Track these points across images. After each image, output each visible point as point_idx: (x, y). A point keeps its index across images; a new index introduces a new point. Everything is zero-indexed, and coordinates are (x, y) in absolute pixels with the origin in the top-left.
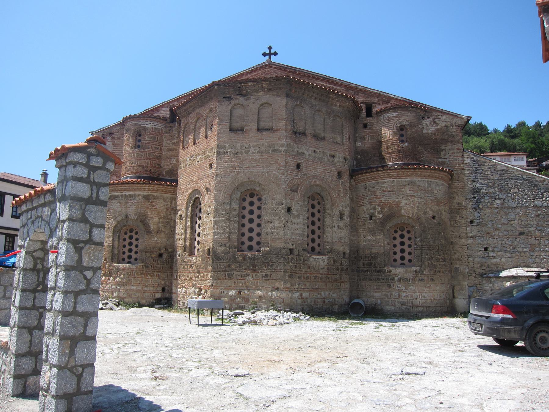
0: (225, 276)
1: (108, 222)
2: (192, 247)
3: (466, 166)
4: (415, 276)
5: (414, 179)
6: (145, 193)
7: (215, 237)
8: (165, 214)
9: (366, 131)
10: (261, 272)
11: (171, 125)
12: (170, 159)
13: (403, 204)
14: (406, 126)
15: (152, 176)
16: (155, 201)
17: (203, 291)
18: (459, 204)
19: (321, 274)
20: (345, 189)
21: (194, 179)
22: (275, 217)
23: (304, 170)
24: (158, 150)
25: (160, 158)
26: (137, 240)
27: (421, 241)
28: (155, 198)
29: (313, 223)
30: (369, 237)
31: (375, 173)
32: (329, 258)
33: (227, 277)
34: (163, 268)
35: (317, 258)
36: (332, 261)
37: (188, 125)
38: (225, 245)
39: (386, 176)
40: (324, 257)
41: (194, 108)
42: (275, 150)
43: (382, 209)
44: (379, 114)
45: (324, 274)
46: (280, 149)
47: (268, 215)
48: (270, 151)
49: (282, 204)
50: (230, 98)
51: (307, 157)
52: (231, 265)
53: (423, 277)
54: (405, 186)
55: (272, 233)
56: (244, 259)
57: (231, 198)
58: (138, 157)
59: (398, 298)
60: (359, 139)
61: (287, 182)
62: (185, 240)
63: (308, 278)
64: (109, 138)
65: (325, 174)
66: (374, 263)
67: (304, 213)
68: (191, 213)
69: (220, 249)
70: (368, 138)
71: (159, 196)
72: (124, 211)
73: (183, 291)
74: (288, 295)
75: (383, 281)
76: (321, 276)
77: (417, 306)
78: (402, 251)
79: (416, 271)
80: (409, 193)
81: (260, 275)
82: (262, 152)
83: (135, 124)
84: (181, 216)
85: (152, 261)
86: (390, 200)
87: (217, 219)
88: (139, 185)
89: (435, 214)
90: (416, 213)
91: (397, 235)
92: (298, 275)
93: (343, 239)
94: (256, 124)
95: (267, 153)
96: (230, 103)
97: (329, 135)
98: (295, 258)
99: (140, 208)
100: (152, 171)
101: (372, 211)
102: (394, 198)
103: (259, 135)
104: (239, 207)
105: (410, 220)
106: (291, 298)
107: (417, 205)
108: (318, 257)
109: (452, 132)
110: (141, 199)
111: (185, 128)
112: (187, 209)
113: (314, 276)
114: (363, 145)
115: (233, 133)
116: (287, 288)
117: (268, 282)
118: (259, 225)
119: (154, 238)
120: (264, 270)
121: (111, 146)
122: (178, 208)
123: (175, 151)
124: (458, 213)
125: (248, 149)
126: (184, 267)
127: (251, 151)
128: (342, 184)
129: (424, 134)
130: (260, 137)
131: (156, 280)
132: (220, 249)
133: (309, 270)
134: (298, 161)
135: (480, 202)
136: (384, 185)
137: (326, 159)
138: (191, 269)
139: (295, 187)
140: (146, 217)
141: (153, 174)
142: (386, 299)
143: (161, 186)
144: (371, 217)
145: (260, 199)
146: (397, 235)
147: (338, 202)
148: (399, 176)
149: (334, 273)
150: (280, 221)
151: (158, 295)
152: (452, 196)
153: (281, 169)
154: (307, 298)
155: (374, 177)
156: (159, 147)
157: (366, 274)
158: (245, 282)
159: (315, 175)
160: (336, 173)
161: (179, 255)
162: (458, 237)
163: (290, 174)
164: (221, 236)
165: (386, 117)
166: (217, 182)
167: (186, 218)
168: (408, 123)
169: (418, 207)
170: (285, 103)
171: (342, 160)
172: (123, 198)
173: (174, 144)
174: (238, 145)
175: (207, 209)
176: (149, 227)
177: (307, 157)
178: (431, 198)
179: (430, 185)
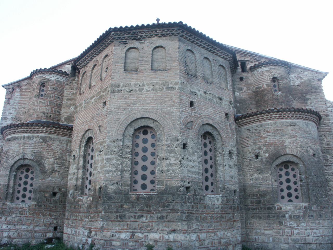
0: (117, 218)
1: (6, 162)
3: (329, 113)
4: (305, 212)
5: (295, 120)
6: (43, 135)
7: (107, 175)
8: (60, 155)
9: (243, 83)
10: (156, 213)
11: (72, 78)
12: (69, 107)
13: (287, 143)
14: (278, 78)
15: (52, 121)
16: (52, 142)
18: (328, 144)
19: (216, 214)
20: (232, 130)
22: (170, 153)
23: (197, 110)
24: (58, 99)
25: (60, 106)
26: (32, 179)
27: (307, 178)
28: (51, 139)
29: (206, 162)
30: (256, 176)
32: (223, 197)
33: (119, 219)
34: (55, 207)
35: (212, 197)
36: (225, 200)
37: (85, 74)
38: (117, 183)
40: (218, 196)
41: (91, 58)
42: (168, 88)
43: (268, 148)
44: (253, 70)
45: (219, 213)
46: (174, 86)
47: (163, 152)
48: (165, 89)
49: (178, 141)
50: (125, 43)
51: (199, 97)
52: (123, 205)
53: (312, 213)
54: (287, 126)
55: (168, 171)
57: (124, 135)
58: (41, 104)
59: (290, 236)
60: (237, 90)
61: (182, 119)
62: (77, 179)
63: (204, 219)
64: (18, 90)
65: (215, 115)
66: (262, 201)
67: (199, 151)
68: (84, 153)
69: (112, 188)
70: (245, 89)
71: (56, 138)
72: (21, 151)
73: (73, 232)
74: (186, 237)
75: (274, 219)
76: (216, 215)
77: (310, 244)
78: (289, 188)
79: (305, 207)
80: (292, 133)
81: (155, 216)
82: (156, 90)
83: (40, 77)
84: (74, 156)
85: (45, 200)
86: (274, 140)
87: (109, 157)
89: (315, 153)
91: (283, 173)
93: (234, 178)
94: (151, 65)
95: (161, 91)
96: (126, 46)
97: (216, 80)
98: (191, 197)
99: (37, 149)
100: (52, 117)
101: (257, 151)
102: (278, 138)
103: (153, 74)
104: (132, 144)
107: (300, 144)
108: (213, 196)
109: (314, 85)
110: (38, 140)
111: (83, 77)
112: (80, 148)
113: (210, 216)
114: (241, 95)
115: (127, 73)
116: (185, 230)
117: (164, 224)
118: (153, 163)
119: (49, 178)
120: (159, 210)
121: (19, 97)
123: (73, 101)
124: (328, 153)
125: (142, 87)
126: (75, 206)
127: (145, 90)
128: (230, 125)
129: (292, 86)
130: (154, 76)
131: (48, 220)
132: (112, 188)
133: (205, 210)
134: (192, 100)
136: (267, 127)
137: (215, 101)
138: (82, 209)
140: (42, 158)
141: (53, 120)
142: (279, 237)
143: (58, 129)
144: (257, 157)
145: (153, 137)
146: (283, 173)
147: (228, 142)
149: (228, 212)
150: (176, 158)
151: (50, 235)
152: (321, 138)
153: (176, 106)
154: (204, 240)
156: (60, 97)
157: (255, 211)
158: (139, 224)
159: (207, 114)
160: (224, 115)
162: (331, 174)
163: (184, 112)
164: (113, 174)
165: (260, 71)
166: (110, 119)
167: (79, 158)
168: (279, 76)
169: (301, 145)
170: (178, 46)
171: (228, 103)
172: (22, 140)
173: (73, 94)
174: (132, 83)
176: (44, 167)
177: (199, 97)
178: (310, 138)
179: (308, 126)
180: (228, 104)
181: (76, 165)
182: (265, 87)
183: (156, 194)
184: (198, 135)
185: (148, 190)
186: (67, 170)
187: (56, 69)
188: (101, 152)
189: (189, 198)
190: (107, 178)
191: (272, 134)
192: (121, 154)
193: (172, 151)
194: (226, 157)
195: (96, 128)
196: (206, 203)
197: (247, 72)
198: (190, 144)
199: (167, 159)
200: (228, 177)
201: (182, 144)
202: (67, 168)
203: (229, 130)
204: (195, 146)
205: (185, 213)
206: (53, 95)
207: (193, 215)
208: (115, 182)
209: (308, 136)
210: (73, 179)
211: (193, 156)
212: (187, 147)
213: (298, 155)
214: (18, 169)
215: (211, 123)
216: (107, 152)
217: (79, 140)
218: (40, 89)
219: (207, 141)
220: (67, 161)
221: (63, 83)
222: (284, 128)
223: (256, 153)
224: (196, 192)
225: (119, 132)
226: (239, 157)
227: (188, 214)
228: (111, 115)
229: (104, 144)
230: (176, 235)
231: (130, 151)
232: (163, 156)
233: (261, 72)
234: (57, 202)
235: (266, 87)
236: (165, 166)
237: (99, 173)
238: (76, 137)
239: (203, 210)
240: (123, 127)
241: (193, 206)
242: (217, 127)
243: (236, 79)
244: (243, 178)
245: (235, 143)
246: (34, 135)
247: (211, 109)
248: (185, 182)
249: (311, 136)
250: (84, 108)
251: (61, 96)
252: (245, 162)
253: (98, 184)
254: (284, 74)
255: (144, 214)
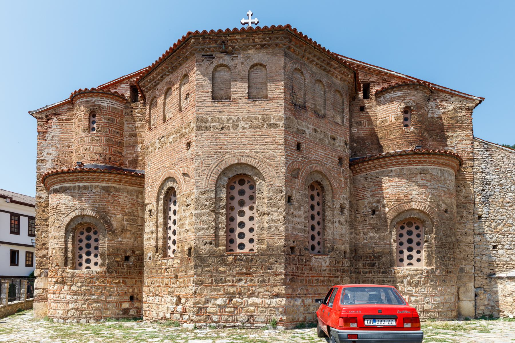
1: (58, 220)
2: (165, 247)
6: (104, 184)
7: (198, 234)
17: (183, 301)
21: (167, 164)
22: (272, 208)
29: (313, 217)
31: (381, 160)
39: (395, 163)
44: (379, 96)
54: (416, 174)
55: (270, 228)
56: (235, 260)
62: (157, 239)
67: (305, 205)
74: (290, 302)
88: (96, 174)
90: (429, 206)
92: (300, 278)
98: (296, 258)
104: (227, 197)
105: (421, 215)
106: (293, 306)
110: (99, 191)
112: (158, 201)
116: (289, 294)
120: (260, 273)
122: (146, 202)
132: (205, 249)
135: (490, 196)
138: (166, 274)
139: (295, 172)
143: (125, 176)
145: (252, 187)
147: (339, 193)
148: (409, 163)
155: (378, 165)
159: (316, 159)
160: (337, 159)
161: (150, 258)
164: (205, 232)
167: (157, 213)
175: (185, 199)
178: (444, 189)
180: (343, 145)
181: (154, 222)
182: (393, 120)
183: (256, 254)
184: (305, 185)
185: (246, 250)
186: (141, 228)
187: (109, 91)
188: (189, 206)
189: (294, 259)
190: (199, 237)
191: (396, 185)
192: (213, 208)
193: (275, 205)
194: (337, 212)
195: (179, 176)
196: (312, 264)
197: (371, 98)
198: (296, 197)
199: (269, 215)
200: (338, 236)
201: (287, 196)
202: (140, 226)
203: (342, 179)
204: (301, 198)
205: (289, 275)
206: (109, 129)
207: (298, 278)
208: (208, 241)
209: (441, 187)
210: (151, 239)
211: (299, 211)
212: (292, 199)
213: (426, 210)
214: (76, 228)
215: (321, 170)
216: (197, 206)
217: (155, 191)
218: (89, 119)
219: (315, 193)
220: (139, 217)
221: (121, 112)
222: (412, 176)
223: (373, 207)
224: (301, 252)
225: (210, 182)
226: (351, 211)
227: (292, 277)
228: (198, 160)
229: (192, 197)
230: (278, 299)
231: (225, 205)
232: (263, 210)
233: (390, 99)
234: (131, 267)
235: (395, 121)
236: (267, 223)
237: (188, 231)
238: (150, 187)
239: (309, 273)
240: (215, 176)
241: (298, 267)
242: (328, 175)
243: (354, 109)
244: (355, 237)
245: (348, 195)
246: (92, 184)
247: (321, 152)
248: (289, 241)
249: (445, 186)
250: (159, 149)
251: (121, 130)
252: (358, 218)
253: (186, 244)
254: (421, 102)
255: (242, 278)
